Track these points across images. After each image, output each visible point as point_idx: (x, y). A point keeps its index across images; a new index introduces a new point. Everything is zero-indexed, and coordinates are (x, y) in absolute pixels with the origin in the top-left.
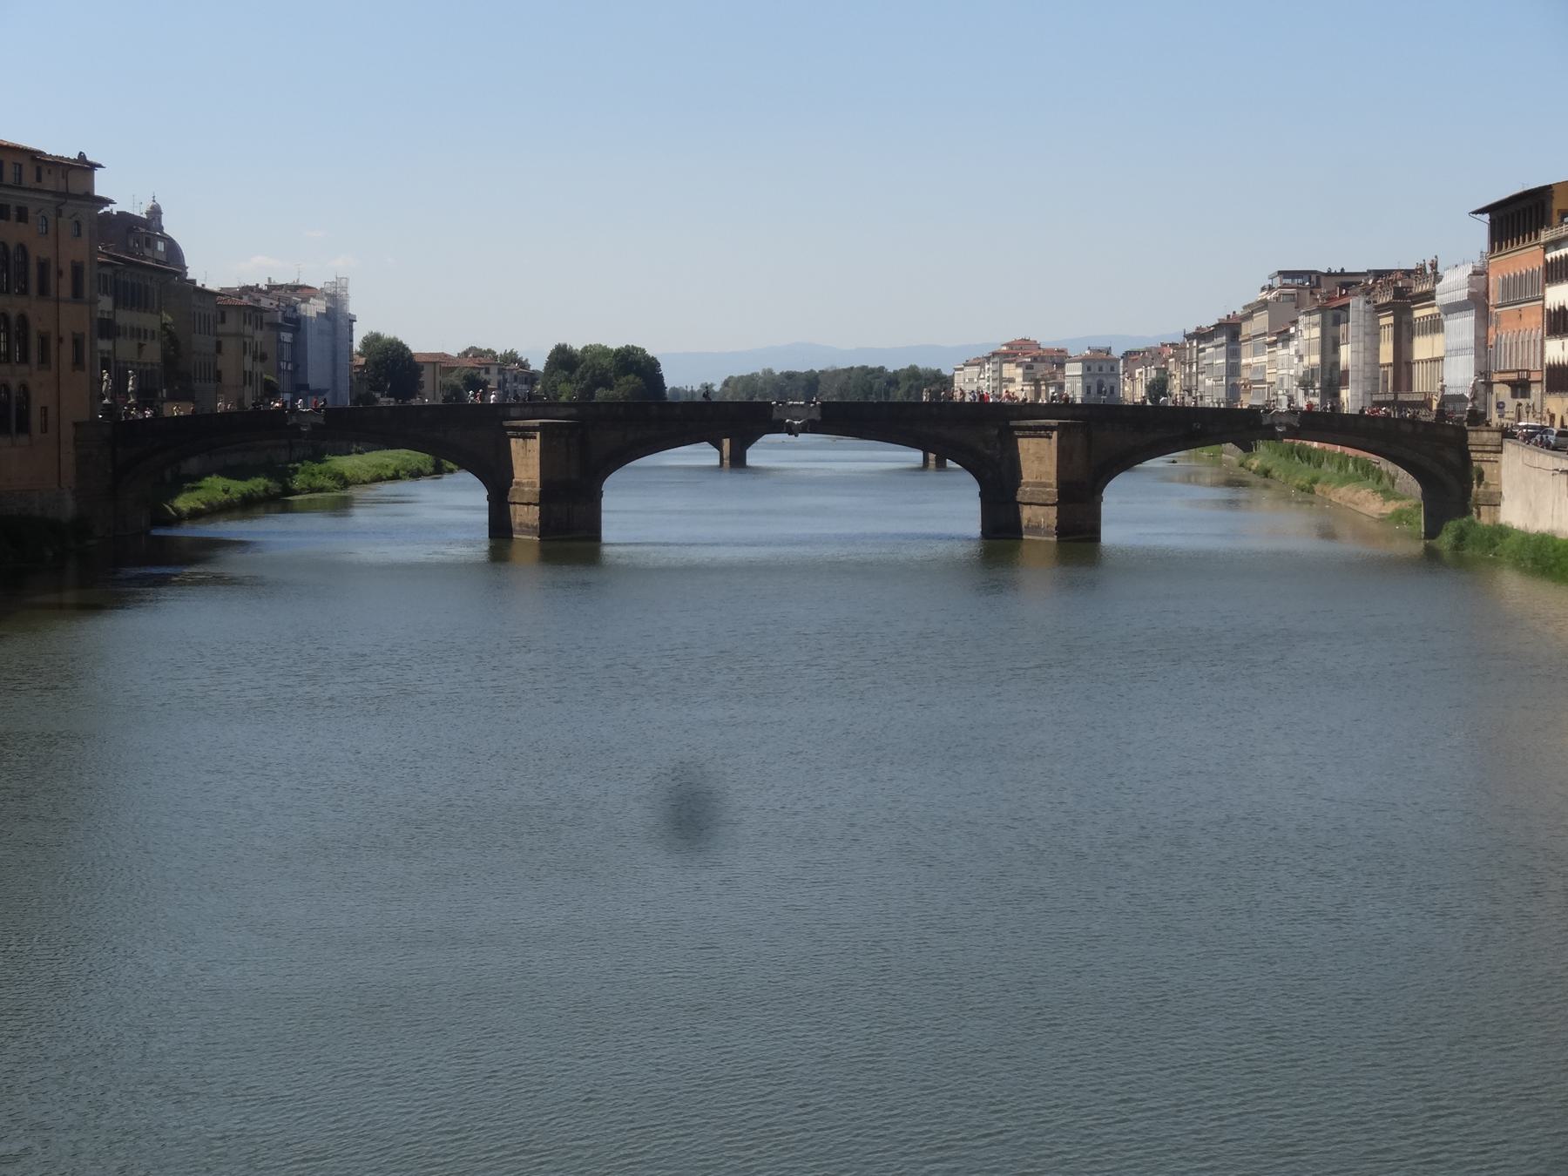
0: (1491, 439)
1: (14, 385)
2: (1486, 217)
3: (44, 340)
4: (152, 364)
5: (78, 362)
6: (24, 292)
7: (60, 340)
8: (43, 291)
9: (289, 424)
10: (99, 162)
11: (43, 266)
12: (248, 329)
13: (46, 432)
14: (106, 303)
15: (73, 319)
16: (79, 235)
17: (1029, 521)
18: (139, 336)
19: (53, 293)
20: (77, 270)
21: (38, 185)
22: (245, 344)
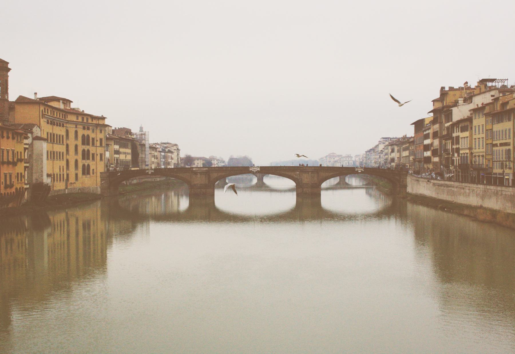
1: (86, 164)
3: (93, 155)
4: (129, 160)
5: (101, 159)
6: (88, 144)
8: (93, 144)
10: (106, 117)
11: (93, 139)
12: (153, 152)
14: (117, 147)
18: (126, 154)
19: (95, 145)
21: (92, 122)
22: (152, 155)
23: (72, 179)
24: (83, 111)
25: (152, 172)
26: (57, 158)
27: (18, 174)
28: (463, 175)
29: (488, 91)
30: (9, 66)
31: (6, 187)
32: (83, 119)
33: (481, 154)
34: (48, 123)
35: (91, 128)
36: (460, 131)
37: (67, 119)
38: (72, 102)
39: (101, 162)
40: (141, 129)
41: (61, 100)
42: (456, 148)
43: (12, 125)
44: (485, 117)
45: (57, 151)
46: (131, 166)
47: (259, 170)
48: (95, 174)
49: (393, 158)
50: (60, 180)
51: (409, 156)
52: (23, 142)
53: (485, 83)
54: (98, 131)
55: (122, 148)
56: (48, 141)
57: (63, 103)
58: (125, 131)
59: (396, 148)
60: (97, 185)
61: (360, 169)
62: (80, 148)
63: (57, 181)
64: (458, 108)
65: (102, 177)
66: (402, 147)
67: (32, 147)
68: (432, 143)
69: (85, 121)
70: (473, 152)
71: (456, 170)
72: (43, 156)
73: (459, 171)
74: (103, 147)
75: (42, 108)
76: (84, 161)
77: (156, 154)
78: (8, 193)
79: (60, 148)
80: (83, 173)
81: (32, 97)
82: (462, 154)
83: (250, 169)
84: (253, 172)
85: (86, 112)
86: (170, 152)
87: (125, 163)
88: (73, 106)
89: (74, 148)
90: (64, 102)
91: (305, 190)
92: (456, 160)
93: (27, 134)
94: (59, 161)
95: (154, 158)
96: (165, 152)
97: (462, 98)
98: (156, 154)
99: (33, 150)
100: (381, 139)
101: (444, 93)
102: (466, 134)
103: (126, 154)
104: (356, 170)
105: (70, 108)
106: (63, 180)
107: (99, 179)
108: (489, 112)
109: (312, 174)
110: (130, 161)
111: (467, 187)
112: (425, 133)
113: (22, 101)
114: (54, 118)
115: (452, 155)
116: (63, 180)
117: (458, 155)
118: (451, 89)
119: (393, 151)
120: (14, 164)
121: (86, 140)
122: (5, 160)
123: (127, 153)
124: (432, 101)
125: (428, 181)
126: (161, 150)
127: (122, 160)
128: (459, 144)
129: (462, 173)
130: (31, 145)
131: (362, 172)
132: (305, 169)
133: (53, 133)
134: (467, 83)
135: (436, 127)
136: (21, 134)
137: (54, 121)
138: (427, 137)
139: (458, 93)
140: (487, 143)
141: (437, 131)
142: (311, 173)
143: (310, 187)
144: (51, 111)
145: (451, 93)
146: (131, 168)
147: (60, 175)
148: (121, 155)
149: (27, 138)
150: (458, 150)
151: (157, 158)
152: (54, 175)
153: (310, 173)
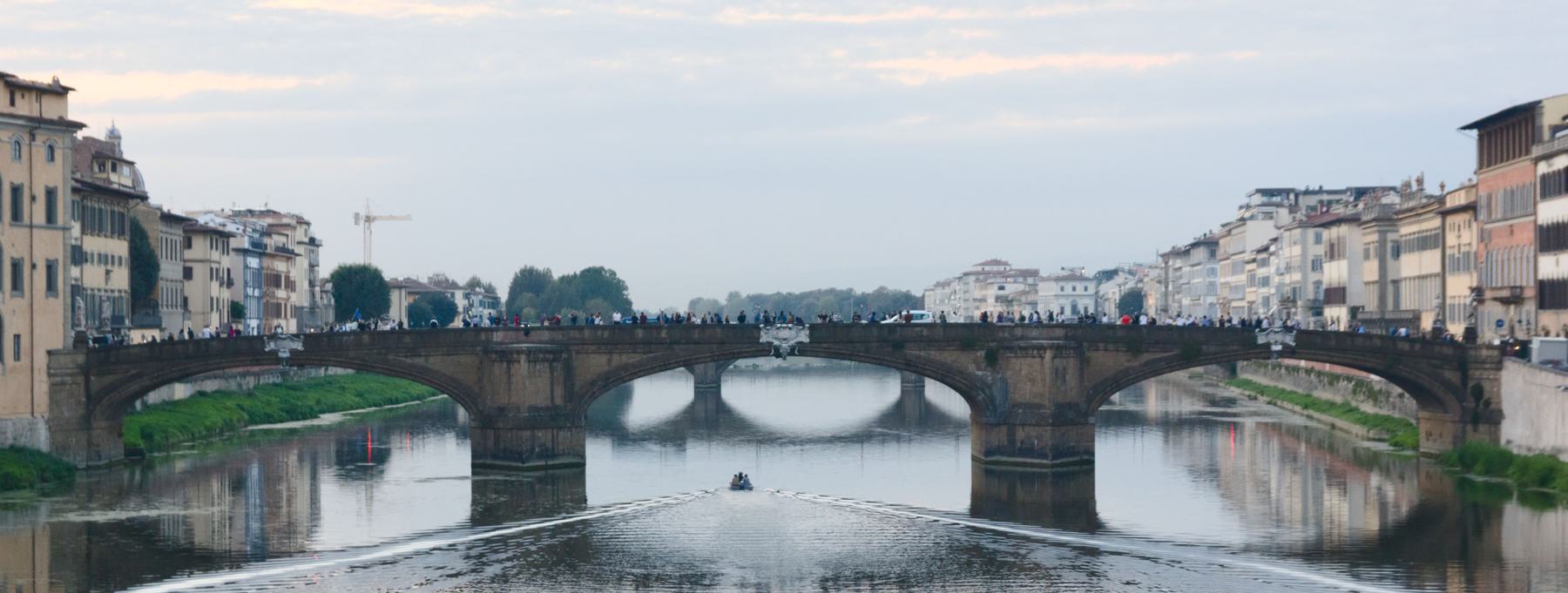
0: (1491, 356)
2: (1474, 133)
3: (16, 266)
4: (120, 291)
5: (51, 286)
7: (34, 266)
8: (16, 216)
9: (267, 350)
12: (215, 255)
15: (49, 246)
16: (52, 158)
17: (1022, 442)
18: (106, 263)
19: (26, 220)
22: (212, 269)
25: (293, 352)
39: (51, 300)
46: (127, 322)
48: (25, 360)
54: (40, 152)
55: (91, 235)
59: (1356, 238)
60: (32, 414)
61: (1279, 337)
65: (55, 375)
66: (1397, 231)
77: (227, 261)
83: (764, 338)
84: (777, 349)
86: (286, 253)
91: (1020, 434)
95: (218, 284)
96: (262, 255)
98: (227, 261)
103: (106, 263)
104: (1261, 340)
109: (1057, 361)
110: (123, 294)
112: (1543, 168)
119: (1334, 252)
123: (113, 257)
126: (246, 245)
127: (92, 290)
132: (1022, 338)
142: (1054, 357)
143: (1050, 421)
146: (130, 329)
148: (87, 267)
151: (230, 284)
153: (1048, 355)
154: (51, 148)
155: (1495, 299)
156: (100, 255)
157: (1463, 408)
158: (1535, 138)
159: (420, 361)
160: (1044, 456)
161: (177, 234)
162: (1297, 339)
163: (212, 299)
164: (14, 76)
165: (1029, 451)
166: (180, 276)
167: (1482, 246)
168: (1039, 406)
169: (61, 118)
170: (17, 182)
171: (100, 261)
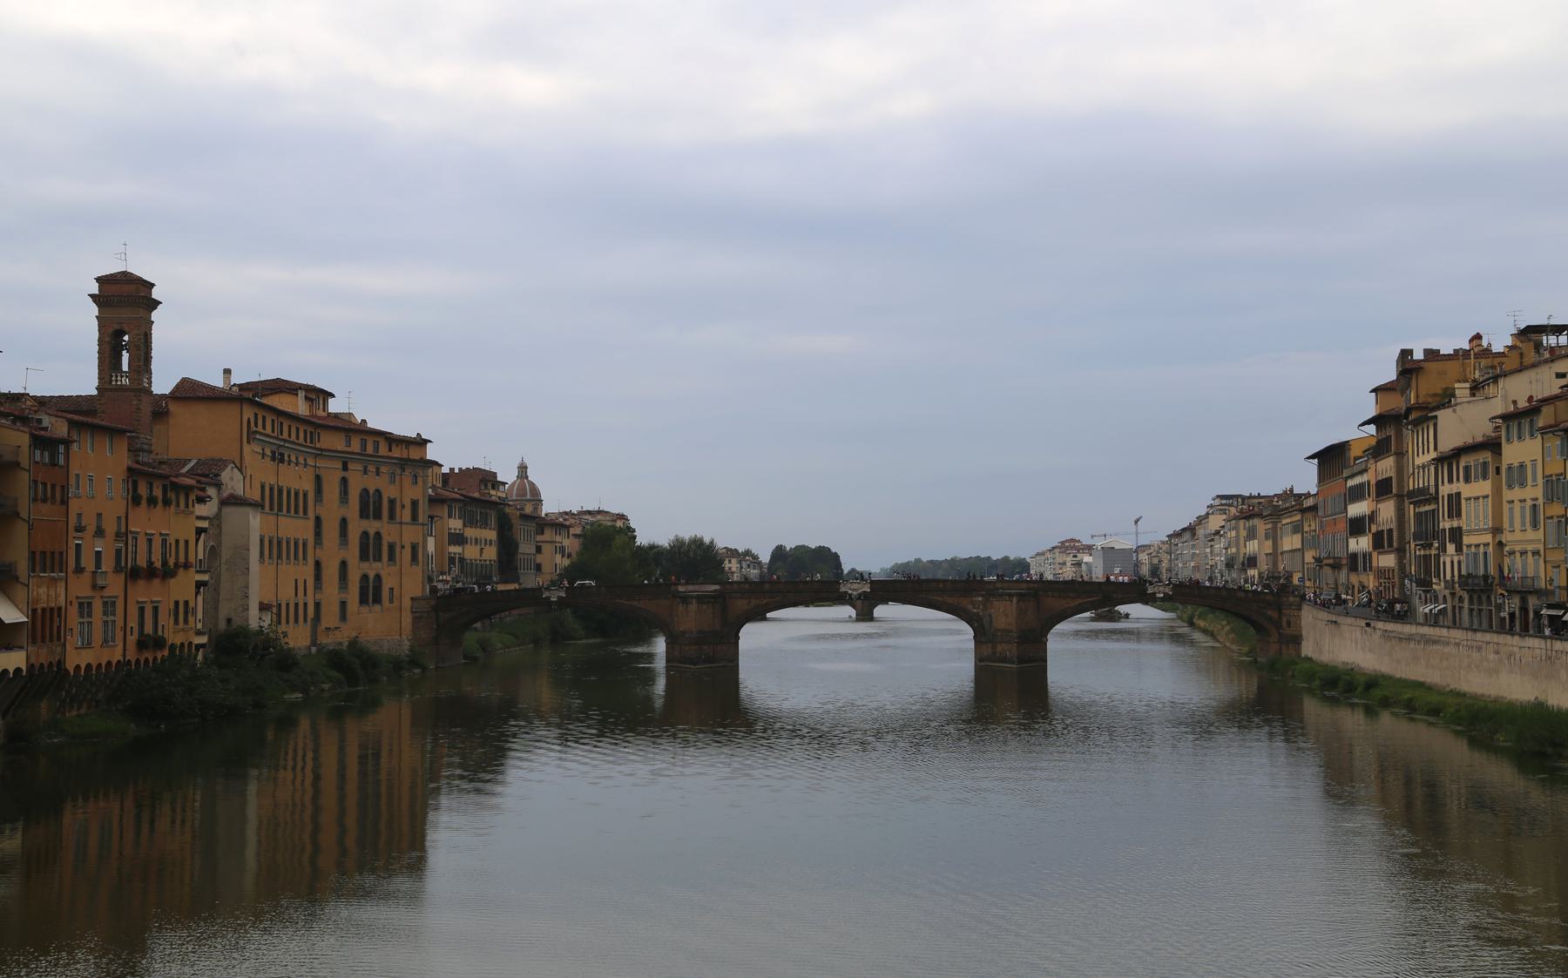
1: (372, 575)
2: (1316, 460)
3: (391, 547)
4: (490, 561)
5: (414, 558)
6: (378, 516)
7: (403, 547)
8: (392, 517)
11: (392, 502)
12: (558, 538)
13: (392, 603)
14: (455, 524)
16: (416, 483)
17: (1000, 654)
19: (398, 520)
20: (414, 504)
21: (390, 454)
22: (556, 547)
23: (330, 618)
24: (364, 421)
25: (559, 598)
26: (288, 558)
27: (177, 603)
28: (1475, 607)
29: (1546, 361)
30: (156, 294)
31: (142, 644)
32: (364, 445)
33: (1530, 547)
34: (264, 455)
35: (384, 469)
36: (1461, 479)
37: (318, 446)
38: (333, 396)
39: (414, 566)
40: (523, 469)
41: (300, 388)
42: (1451, 529)
43: (161, 463)
44: (1539, 437)
45: (289, 536)
46: (495, 579)
47: (869, 590)
48: (396, 603)
49: (1252, 555)
50: (296, 621)
51: (1302, 550)
52: (192, 513)
53: (1534, 337)
54: (407, 480)
56: (263, 507)
57: (306, 398)
58: (480, 477)
59: (1261, 526)
60: (401, 635)
61: (1161, 589)
62: (356, 527)
63: (288, 622)
64: (1454, 411)
66: (1281, 522)
67: (219, 526)
68: (1373, 512)
69: (370, 450)
70: (1504, 541)
71: (1453, 594)
72: (248, 550)
73: (1461, 597)
74: (418, 524)
75: (248, 413)
76: (365, 565)
78: (147, 660)
79: (296, 528)
80: (363, 600)
81: (217, 381)
82: (1469, 546)
83: (843, 589)
84: (850, 595)
85: (371, 425)
87: (479, 570)
88: (334, 406)
89: (337, 525)
90: (311, 396)
91: (999, 648)
92: (1452, 562)
93: (203, 490)
94: (294, 564)
97: (1465, 381)
98: (566, 542)
99: (220, 534)
100: (1214, 500)
101: (1408, 367)
102: (1483, 487)
104: (1150, 591)
105: (325, 414)
106: (305, 620)
107: (407, 619)
108: (1553, 422)
111: (1491, 645)
112: (1350, 483)
113: (189, 392)
114: (282, 443)
115: (1438, 548)
116: (305, 620)
117: (1459, 549)
118: (1432, 354)
119: (1251, 535)
120: (167, 573)
121: (371, 506)
122: (142, 562)
123: (486, 540)
124: (1371, 392)
125: (1368, 625)
127: (471, 560)
128: (1459, 515)
129: (1471, 602)
130: (216, 520)
131: (1167, 598)
133: (278, 486)
134: (1478, 337)
135: (1386, 466)
136: (187, 490)
137: (282, 450)
138: (1357, 494)
139: (1453, 368)
140: (1548, 514)
141: (1391, 477)
142: (1018, 602)
144: (273, 421)
145: (1432, 366)
146: (497, 583)
147: (297, 605)
148: (468, 547)
149: (201, 500)
150: (1456, 535)
151: (569, 556)
152: (279, 606)
154: (416, 477)
155: (1326, 565)
156: (476, 539)
157: (1280, 634)
158: (1345, 465)
159: (635, 603)
160: (1013, 663)
161: (532, 526)
162: (1172, 589)
163: (556, 564)
164: (391, 434)
165: (1004, 660)
166: (534, 551)
167: (1321, 532)
168: (1011, 631)
169: (422, 458)
170: (392, 497)
171: (476, 543)
